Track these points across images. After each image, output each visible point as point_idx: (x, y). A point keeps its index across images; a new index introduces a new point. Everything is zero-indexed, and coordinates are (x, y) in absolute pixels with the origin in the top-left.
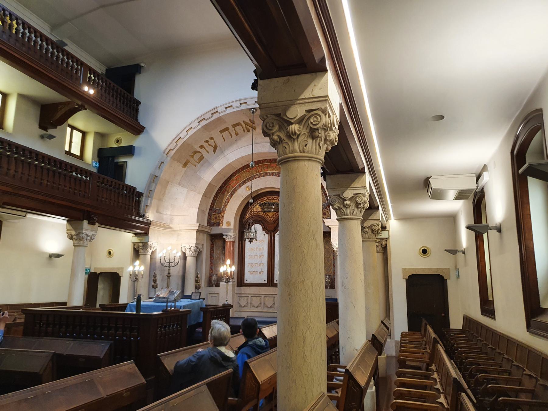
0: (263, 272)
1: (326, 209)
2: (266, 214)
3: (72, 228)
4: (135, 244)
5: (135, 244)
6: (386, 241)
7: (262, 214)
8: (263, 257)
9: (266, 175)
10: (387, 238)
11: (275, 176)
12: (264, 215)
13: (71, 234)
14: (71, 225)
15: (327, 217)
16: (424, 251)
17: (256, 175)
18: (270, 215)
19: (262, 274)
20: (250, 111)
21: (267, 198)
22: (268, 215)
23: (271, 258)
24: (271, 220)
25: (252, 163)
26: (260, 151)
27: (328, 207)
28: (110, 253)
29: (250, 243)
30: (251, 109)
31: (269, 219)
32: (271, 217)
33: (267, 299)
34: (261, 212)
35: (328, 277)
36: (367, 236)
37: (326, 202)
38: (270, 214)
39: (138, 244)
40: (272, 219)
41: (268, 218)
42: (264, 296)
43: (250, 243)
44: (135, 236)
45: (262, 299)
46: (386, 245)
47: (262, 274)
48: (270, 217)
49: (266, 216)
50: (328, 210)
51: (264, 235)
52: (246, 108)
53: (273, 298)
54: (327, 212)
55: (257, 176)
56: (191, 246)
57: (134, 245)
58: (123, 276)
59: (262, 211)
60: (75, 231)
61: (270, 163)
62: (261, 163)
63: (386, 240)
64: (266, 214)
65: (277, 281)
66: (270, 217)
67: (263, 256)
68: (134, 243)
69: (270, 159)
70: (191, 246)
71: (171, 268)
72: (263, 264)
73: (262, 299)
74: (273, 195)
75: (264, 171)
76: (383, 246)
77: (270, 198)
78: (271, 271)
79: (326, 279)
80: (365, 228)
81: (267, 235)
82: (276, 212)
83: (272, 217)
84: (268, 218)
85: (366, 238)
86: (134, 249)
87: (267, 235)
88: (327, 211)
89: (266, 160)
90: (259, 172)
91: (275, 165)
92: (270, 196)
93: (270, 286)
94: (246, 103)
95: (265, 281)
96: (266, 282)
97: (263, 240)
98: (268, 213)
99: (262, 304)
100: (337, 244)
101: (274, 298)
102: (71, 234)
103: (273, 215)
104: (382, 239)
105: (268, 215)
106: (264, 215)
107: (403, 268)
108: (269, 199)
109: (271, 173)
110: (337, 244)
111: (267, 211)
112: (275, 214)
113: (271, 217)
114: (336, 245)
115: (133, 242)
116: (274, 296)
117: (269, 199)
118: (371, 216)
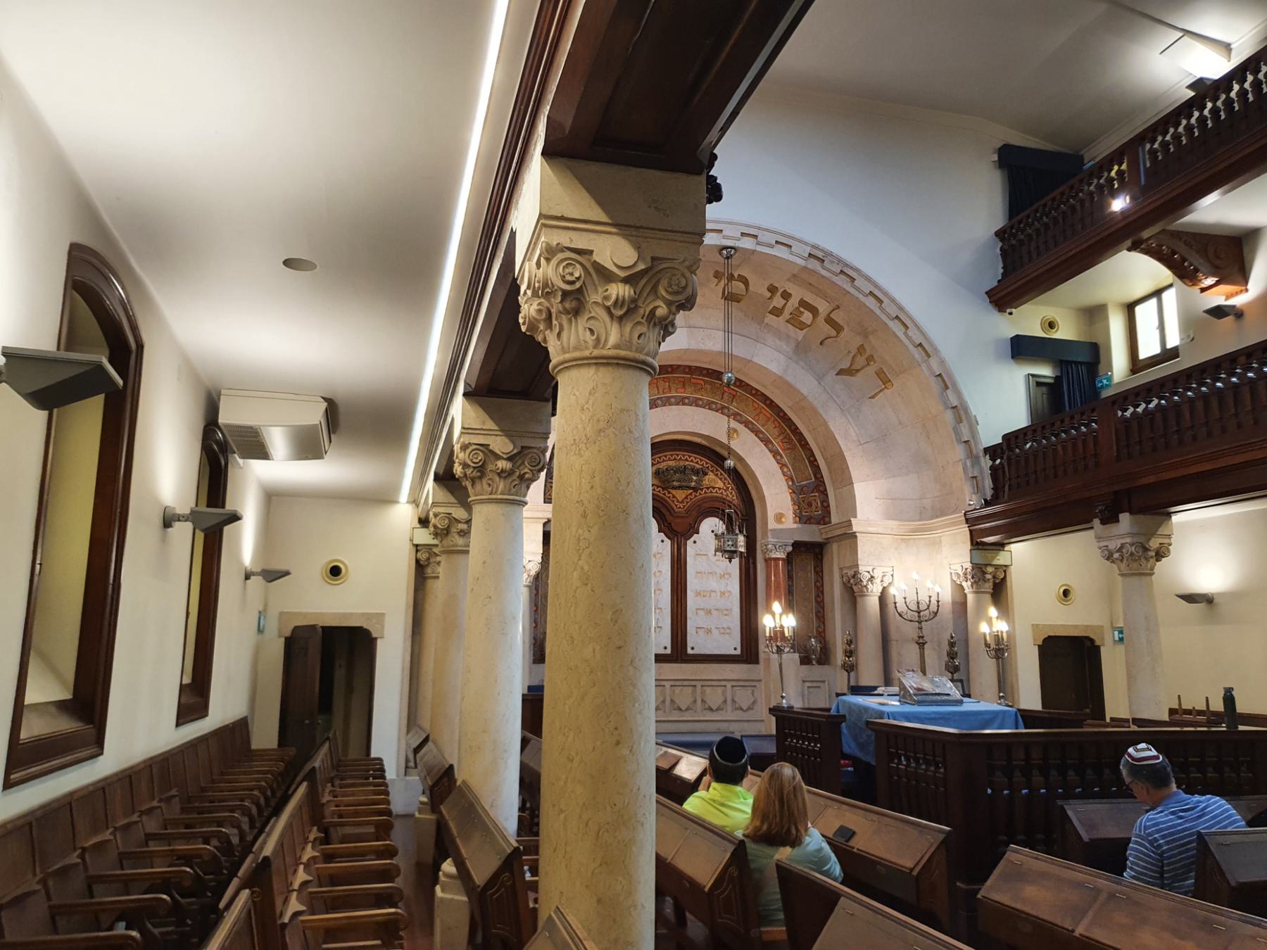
0: (660, 627)
1: (812, 492)
2: (669, 493)
3: (456, 501)
4: (419, 548)
5: (419, 548)
6: (1005, 571)
7: (659, 492)
8: (660, 592)
9: (681, 401)
10: (1006, 566)
11: (700, 406)
12: (664, 494)
13: (448, 518)
14: (452, 493)
15: (816, 511)
16: (1066, 593)
17: (658, 398)
18: (677, 496)
19: (659, 632)
20: (720, 254)
21: (672, 455)
22: (674, 496)
23: (679, 598)
24: (680, 508)
25: (730, 375)
26: (702, 347)
27: (815, 491)
28: (335, 571)
29: (730, 562)
30: (726, 248)
31: (676, 506)
32: (680, 500)
33: (677, 690)
34: (658, 487)
35: (813, 640)
36: (1149, 566)
37: (811, 479)
38: (680, 495)
39: (431, 549)
40: (684, 506)
41: (673, 501)
42: (673, 683)
43: (730, 562)
44: (423, 527)
45: (668, 691)
46: (1004, 579)
47: (659, 632)
48: (678, 501)
49: (669, 497)
50: (815, 496)
51: (663, 541)
52: (717, 243)
53: (691, 688)
54: (815, 500)
55: (659, 402)
56: (529, 561)
57: (417, 551)
58: (382, 638)
59: (659, 484)
60: (466, 510)
61: (689, 376)
62: (668, 373)
63: (1004, 568)
64: (669, 493)
65: (693, 648)
66: (678, 501)
67: (660, 590)
68: (417, 546)
69: (690, 367)
70: (529, 561)
71: (922, 623)
72: (661, 609)
73: (668, 691)
74: (686, 451)
75: (676, 392)
76: (997, 581)
77: (678, 455)
78: (679, 624)
79: (813, 645)
80: (1150, 550)
81: (668, 542)
82: (691, 491)
83: (682, 502)
84: (673, 501)
85: (1147, 569)
86: (417, 561)
87: (669, 542)
88: (814, 498)
89: (679, 366)
90: (664, 393)
91: (703, 383)
92: (678, 453)
93: (677, 660)
94: (721, 231)
95: (665, 648)
96: (669, 651)
97: (660, 553)
98: (674, 492)
99: (668, 702)
100: (869, 572)
101: (693, 688)
102: (448, 518)
103: (686, 498)
104: (997, 567)
105: (673, 495)
106: (664, 494)
107: (1033, 625)
108: (675, 459)
109: (691, 399)
110: (869, 572)
111: (675, 488)
112: (691, 494)
113: (680, 500)
114: (867, 574)
115: (415, 543)
116: (723, 683)
117: (675, 459)
118: (1160, 529)
